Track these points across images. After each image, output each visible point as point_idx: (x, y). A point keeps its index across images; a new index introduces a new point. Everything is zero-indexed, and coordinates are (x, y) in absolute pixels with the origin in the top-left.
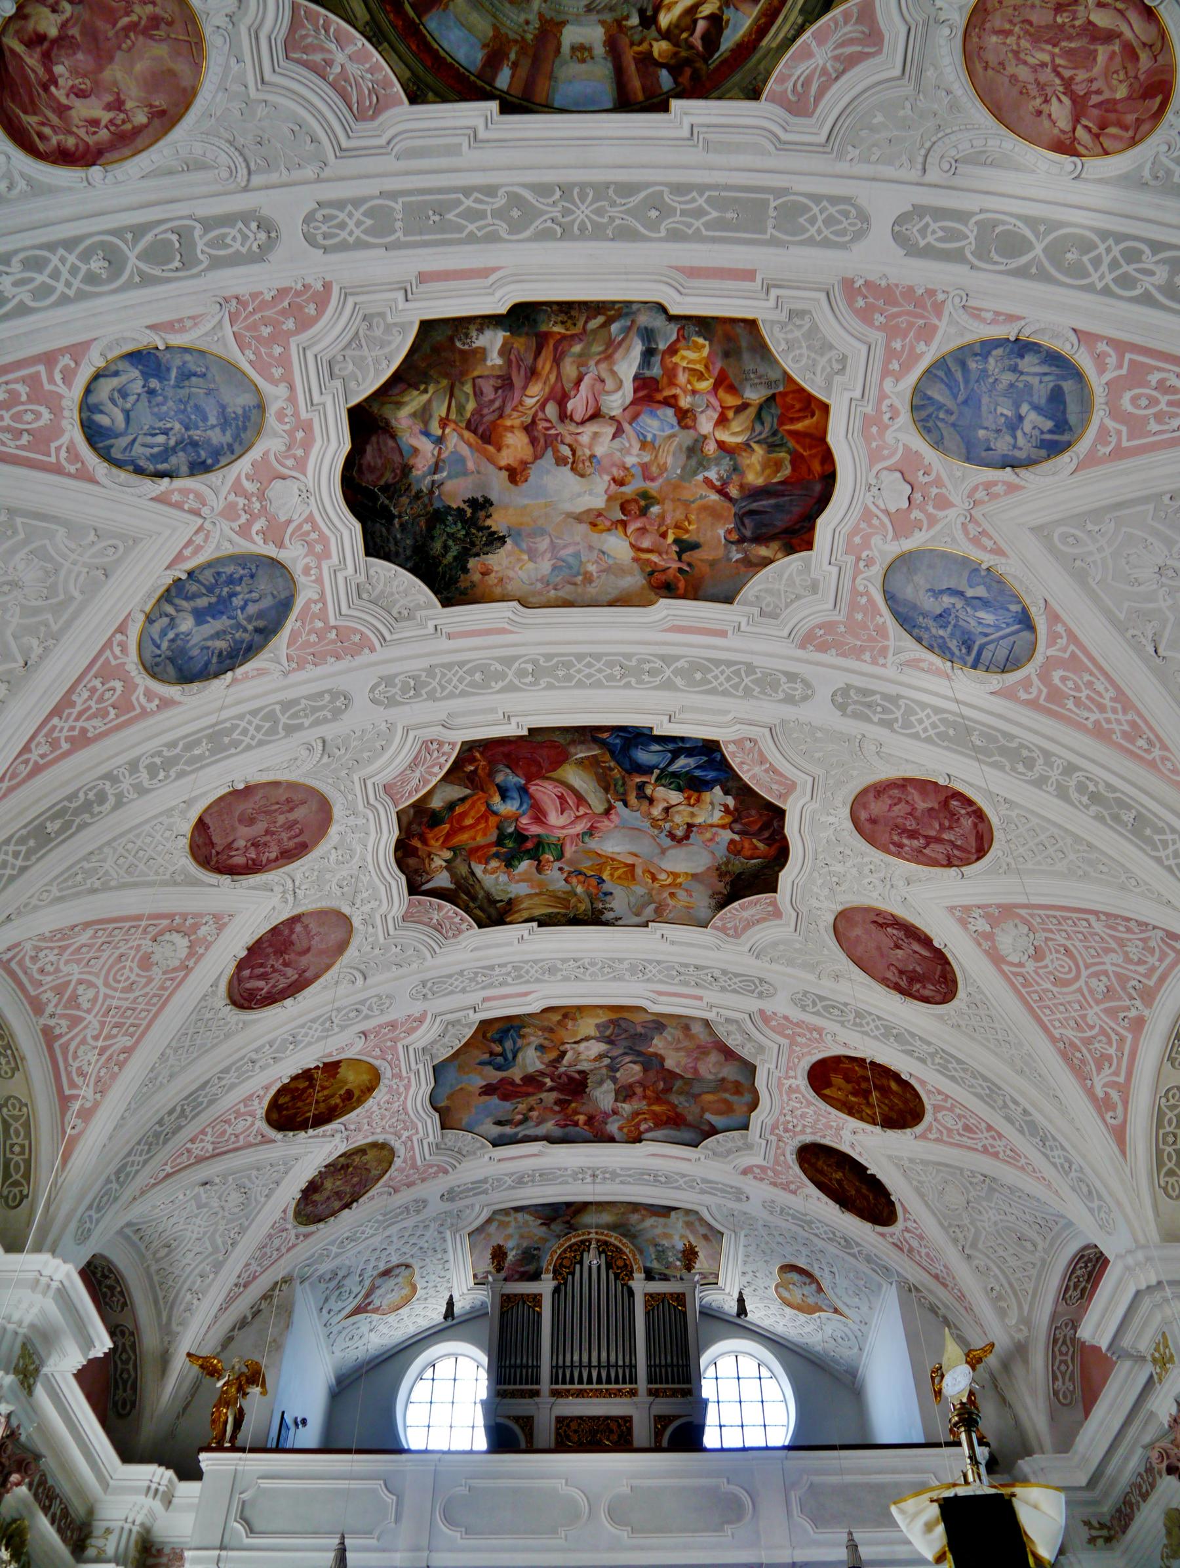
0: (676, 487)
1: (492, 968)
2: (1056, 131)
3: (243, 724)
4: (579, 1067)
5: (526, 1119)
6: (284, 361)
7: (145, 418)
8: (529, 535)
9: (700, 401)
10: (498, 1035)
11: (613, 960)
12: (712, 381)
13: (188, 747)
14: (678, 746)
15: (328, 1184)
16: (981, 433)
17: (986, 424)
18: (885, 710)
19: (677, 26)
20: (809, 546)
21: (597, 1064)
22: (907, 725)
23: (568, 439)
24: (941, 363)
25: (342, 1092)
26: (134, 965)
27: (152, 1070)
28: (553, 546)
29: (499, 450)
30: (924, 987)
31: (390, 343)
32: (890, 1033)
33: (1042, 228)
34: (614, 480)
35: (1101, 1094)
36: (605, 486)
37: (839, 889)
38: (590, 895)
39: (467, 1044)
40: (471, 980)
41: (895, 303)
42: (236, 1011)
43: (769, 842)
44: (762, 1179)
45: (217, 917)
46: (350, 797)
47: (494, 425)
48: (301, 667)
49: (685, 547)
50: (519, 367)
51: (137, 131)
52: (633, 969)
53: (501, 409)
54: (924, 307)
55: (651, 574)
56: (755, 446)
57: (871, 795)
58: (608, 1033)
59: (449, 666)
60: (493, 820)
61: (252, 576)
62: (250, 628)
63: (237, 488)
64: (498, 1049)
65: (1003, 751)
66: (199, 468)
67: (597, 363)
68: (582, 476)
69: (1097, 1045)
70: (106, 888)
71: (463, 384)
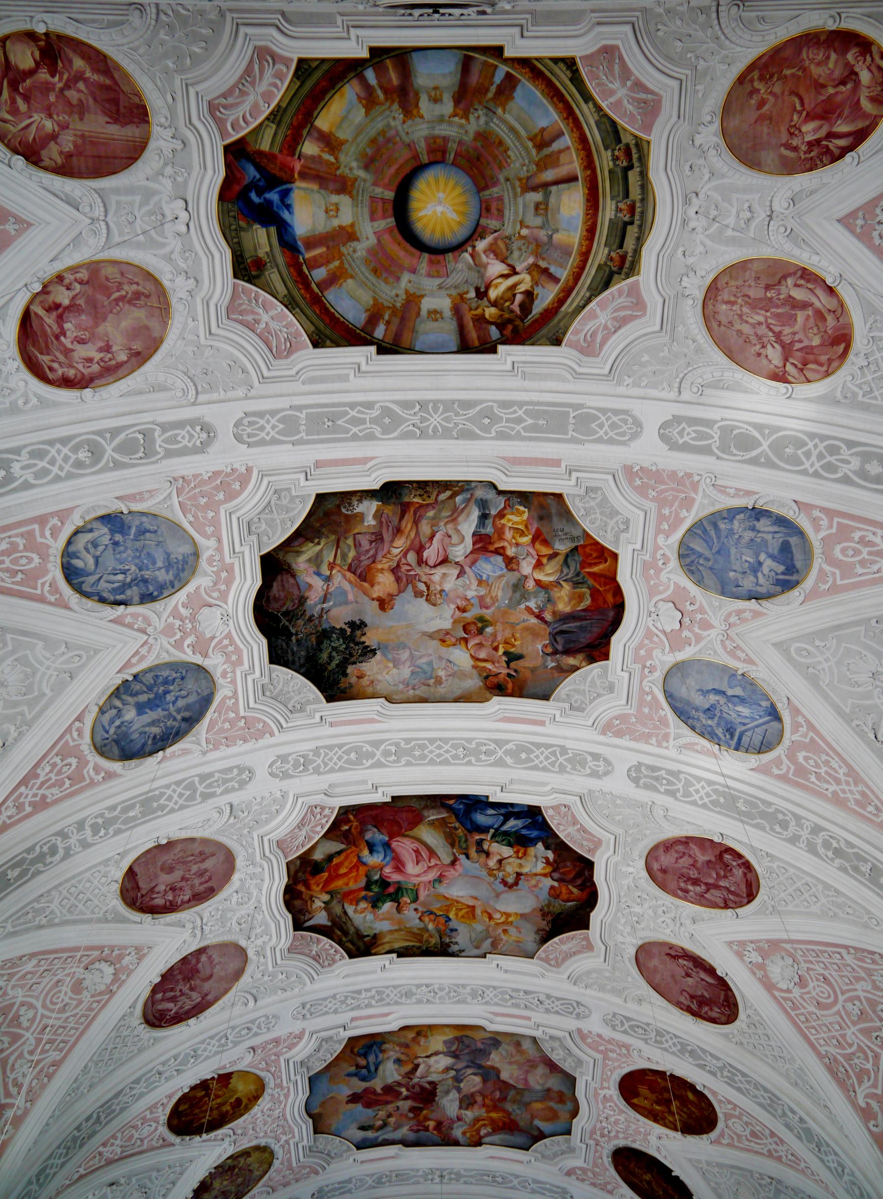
0: (505, 613)
1: (359, 992)
2: (772, 367)
3: (169, 792)
4: (429, 1079)
5: (385, 1125)
7: (110, 561)
8: (393, 649)
9: (523, 551)
10: (364, 1049)
11: (458, 986)
13: (125, 810)
14: (508, 810)
15: (217, 1184)
16: (732, 574)
18: (669, 783)
19: (502, 298)
20: (606, 657)
21: (444, 1076)
22: (687, 794)
23: (424, 579)
25: (233, 1100)
26: (69, 990)
27: (75, 1081)
28: (412, 657)
29: (372, 586)
30: (711, 1009)
31: (293, 509)
32: (685, 1049)
33: (767, 431)
34: (458, 608)
35: (862, 1103)
36: (450, 613)
37: (639, 927)
38: (439, 931)
39: (338, 1058)
40: (342, 1002)
41: (663, 482)
42: (148, 1029)
43: (581, 887)
44: (583, 1180)
45: (138, 949)
46: (250, 851)
47: (369, 568)
48: (216, 748)
49: (512, 658)
51: (120, 365)
52: (474, 994)
53: (374, 556)
54: (684, 485)
55: (487, 678)
56: (563, 583)
57: (661, 850)
58: (453, 1049)
59: (330, 748)
60: (362, 870)
61: (183, 678)
62: (179, 717)
64: (363, 1062)
65: (763, 815)
66: (147, 598)
67: (446, 524)
68: (434, 605)
69: (856, 1061)
70: (51, 925)
71: (346, 538)
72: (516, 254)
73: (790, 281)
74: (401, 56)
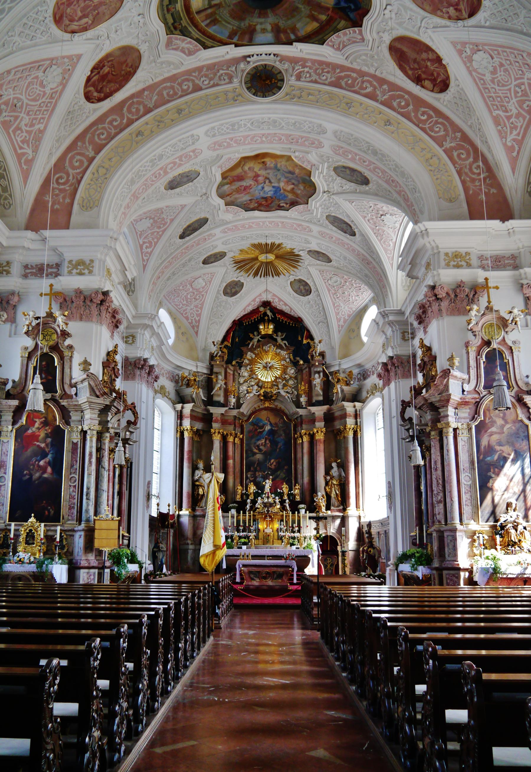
74: (278, 42)
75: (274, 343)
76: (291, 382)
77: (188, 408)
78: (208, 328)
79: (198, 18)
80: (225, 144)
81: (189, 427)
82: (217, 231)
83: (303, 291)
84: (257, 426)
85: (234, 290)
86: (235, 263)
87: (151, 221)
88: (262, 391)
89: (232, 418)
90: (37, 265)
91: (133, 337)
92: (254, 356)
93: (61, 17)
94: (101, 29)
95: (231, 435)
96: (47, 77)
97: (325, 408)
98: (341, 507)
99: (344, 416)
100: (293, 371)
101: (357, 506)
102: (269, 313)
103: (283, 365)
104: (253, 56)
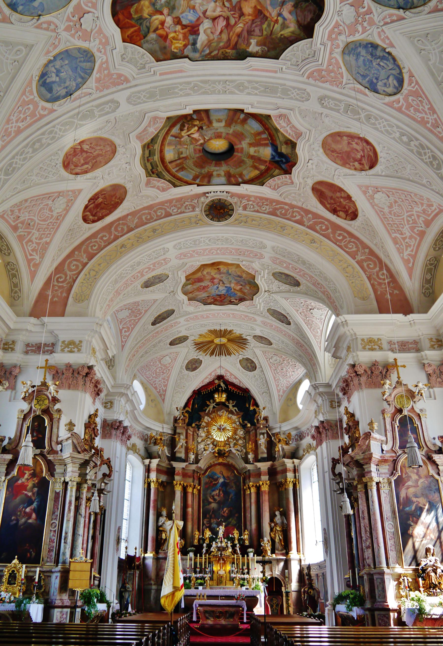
6: (330, 64)
9: (172, 29)
12: (169, 37)
17: (67, 66)
23: (226, 9)
24: (90, 75)
29: (255, 7)
31: (291, 55)
41: (111, 83)
50: (244, 38)
54: (102, 86)
56: (148, 16)
63: (364, 30)
67: (214, 39)
71: (267, 35)
72: (188, 140)
73: (90, 167)
74: (230, 183)
75: (227, 409)
76: (240, 442)
77: (155, 462)
78: (173, 396)
79: (170, 166)
80: (189, 255)
81: (155, 479)
82: (182, 320)
83: (250, 367)
84: (213, 478)
85: (194, 366)
86: (195, 345)
87: (130, 311)
88: (216, 449)
89: (192, 472)
90: (36, 344)
91: (112, 403)
92: (210, 420)
93: (68, 164)
94: (98, 172)
95: (190, 486)
96: (55, 204)
97: (269, 464)
98: (284, 551)
99: (285, 471)
100: (242, 433)
101: (298, 551)
102: (222, 385)
103: (234, 427)
104: (211, 192)
